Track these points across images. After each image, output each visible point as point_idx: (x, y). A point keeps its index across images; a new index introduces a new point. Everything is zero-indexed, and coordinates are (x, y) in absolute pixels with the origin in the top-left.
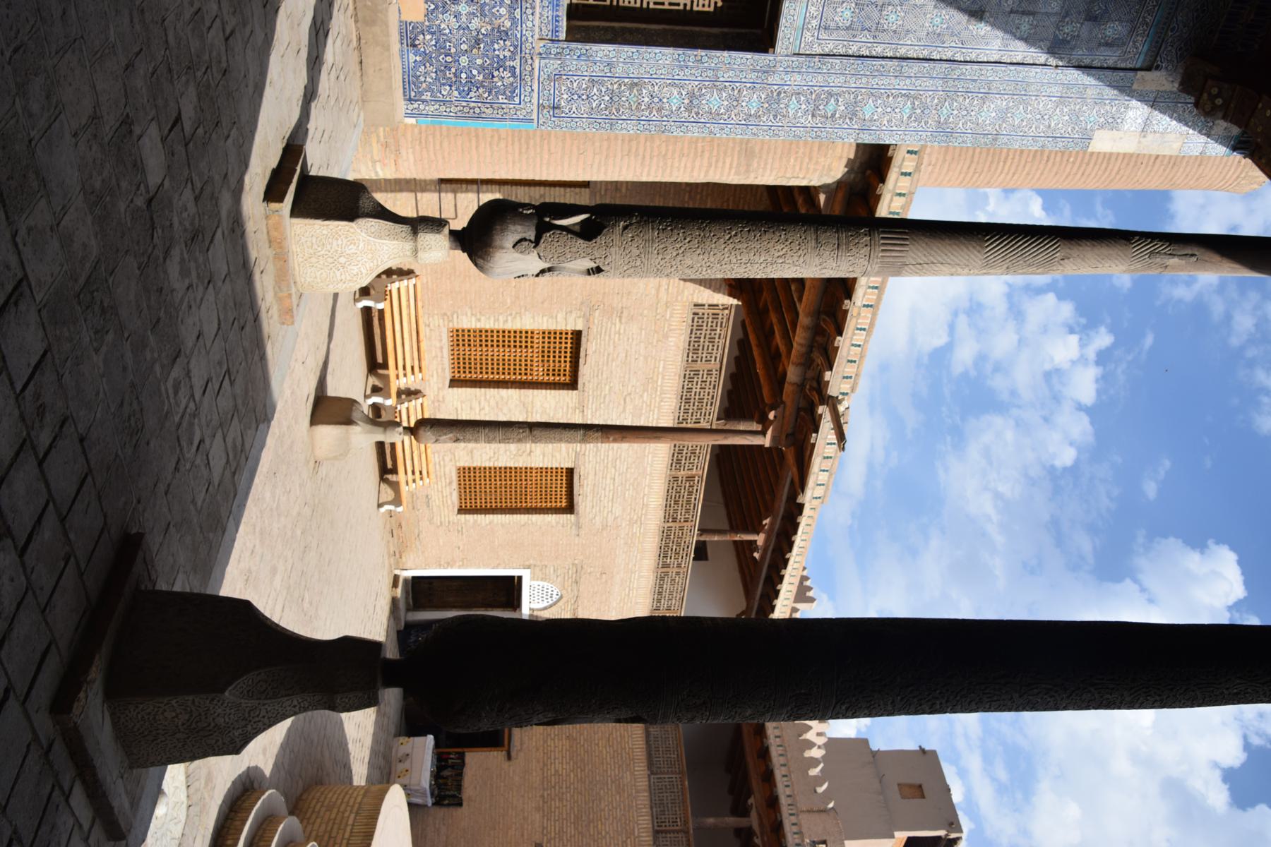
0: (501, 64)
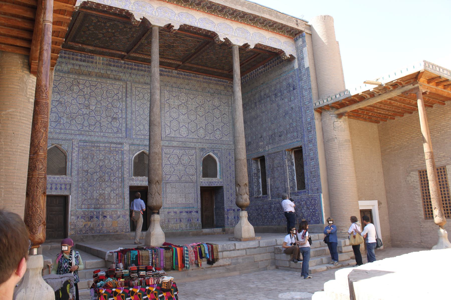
0: (311, 202)
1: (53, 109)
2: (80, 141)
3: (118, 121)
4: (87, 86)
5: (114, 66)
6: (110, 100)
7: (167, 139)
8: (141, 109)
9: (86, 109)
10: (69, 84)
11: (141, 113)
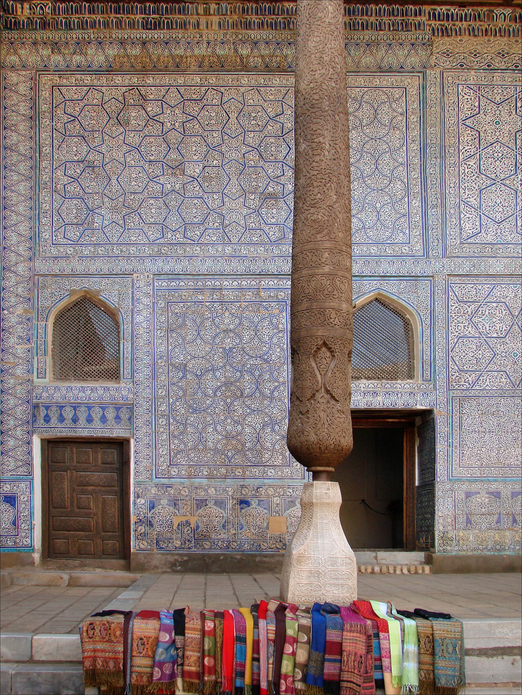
1: (69, 188)
2: (158, 275)
3: (281, 204)
4: (173, 103)
5: (261, 26)
6: (252, 139)
7: (467, 250)
8: (367, 158)
9: (174, 174)
10: (113, 107)
11: (368, 171)
